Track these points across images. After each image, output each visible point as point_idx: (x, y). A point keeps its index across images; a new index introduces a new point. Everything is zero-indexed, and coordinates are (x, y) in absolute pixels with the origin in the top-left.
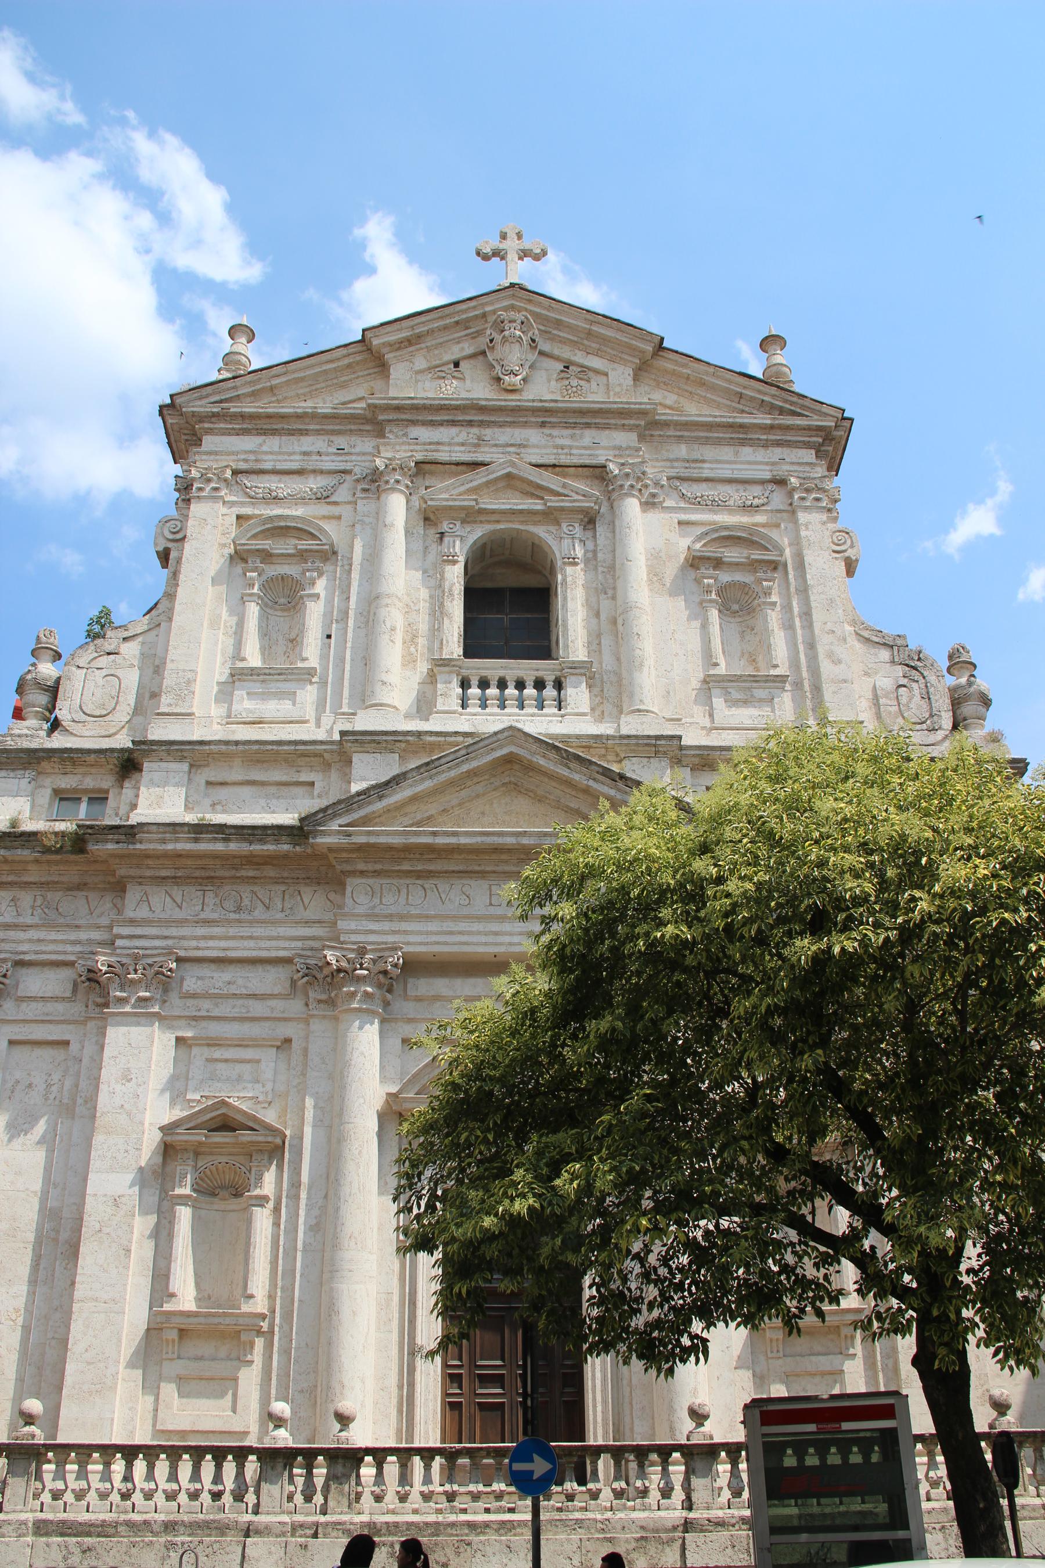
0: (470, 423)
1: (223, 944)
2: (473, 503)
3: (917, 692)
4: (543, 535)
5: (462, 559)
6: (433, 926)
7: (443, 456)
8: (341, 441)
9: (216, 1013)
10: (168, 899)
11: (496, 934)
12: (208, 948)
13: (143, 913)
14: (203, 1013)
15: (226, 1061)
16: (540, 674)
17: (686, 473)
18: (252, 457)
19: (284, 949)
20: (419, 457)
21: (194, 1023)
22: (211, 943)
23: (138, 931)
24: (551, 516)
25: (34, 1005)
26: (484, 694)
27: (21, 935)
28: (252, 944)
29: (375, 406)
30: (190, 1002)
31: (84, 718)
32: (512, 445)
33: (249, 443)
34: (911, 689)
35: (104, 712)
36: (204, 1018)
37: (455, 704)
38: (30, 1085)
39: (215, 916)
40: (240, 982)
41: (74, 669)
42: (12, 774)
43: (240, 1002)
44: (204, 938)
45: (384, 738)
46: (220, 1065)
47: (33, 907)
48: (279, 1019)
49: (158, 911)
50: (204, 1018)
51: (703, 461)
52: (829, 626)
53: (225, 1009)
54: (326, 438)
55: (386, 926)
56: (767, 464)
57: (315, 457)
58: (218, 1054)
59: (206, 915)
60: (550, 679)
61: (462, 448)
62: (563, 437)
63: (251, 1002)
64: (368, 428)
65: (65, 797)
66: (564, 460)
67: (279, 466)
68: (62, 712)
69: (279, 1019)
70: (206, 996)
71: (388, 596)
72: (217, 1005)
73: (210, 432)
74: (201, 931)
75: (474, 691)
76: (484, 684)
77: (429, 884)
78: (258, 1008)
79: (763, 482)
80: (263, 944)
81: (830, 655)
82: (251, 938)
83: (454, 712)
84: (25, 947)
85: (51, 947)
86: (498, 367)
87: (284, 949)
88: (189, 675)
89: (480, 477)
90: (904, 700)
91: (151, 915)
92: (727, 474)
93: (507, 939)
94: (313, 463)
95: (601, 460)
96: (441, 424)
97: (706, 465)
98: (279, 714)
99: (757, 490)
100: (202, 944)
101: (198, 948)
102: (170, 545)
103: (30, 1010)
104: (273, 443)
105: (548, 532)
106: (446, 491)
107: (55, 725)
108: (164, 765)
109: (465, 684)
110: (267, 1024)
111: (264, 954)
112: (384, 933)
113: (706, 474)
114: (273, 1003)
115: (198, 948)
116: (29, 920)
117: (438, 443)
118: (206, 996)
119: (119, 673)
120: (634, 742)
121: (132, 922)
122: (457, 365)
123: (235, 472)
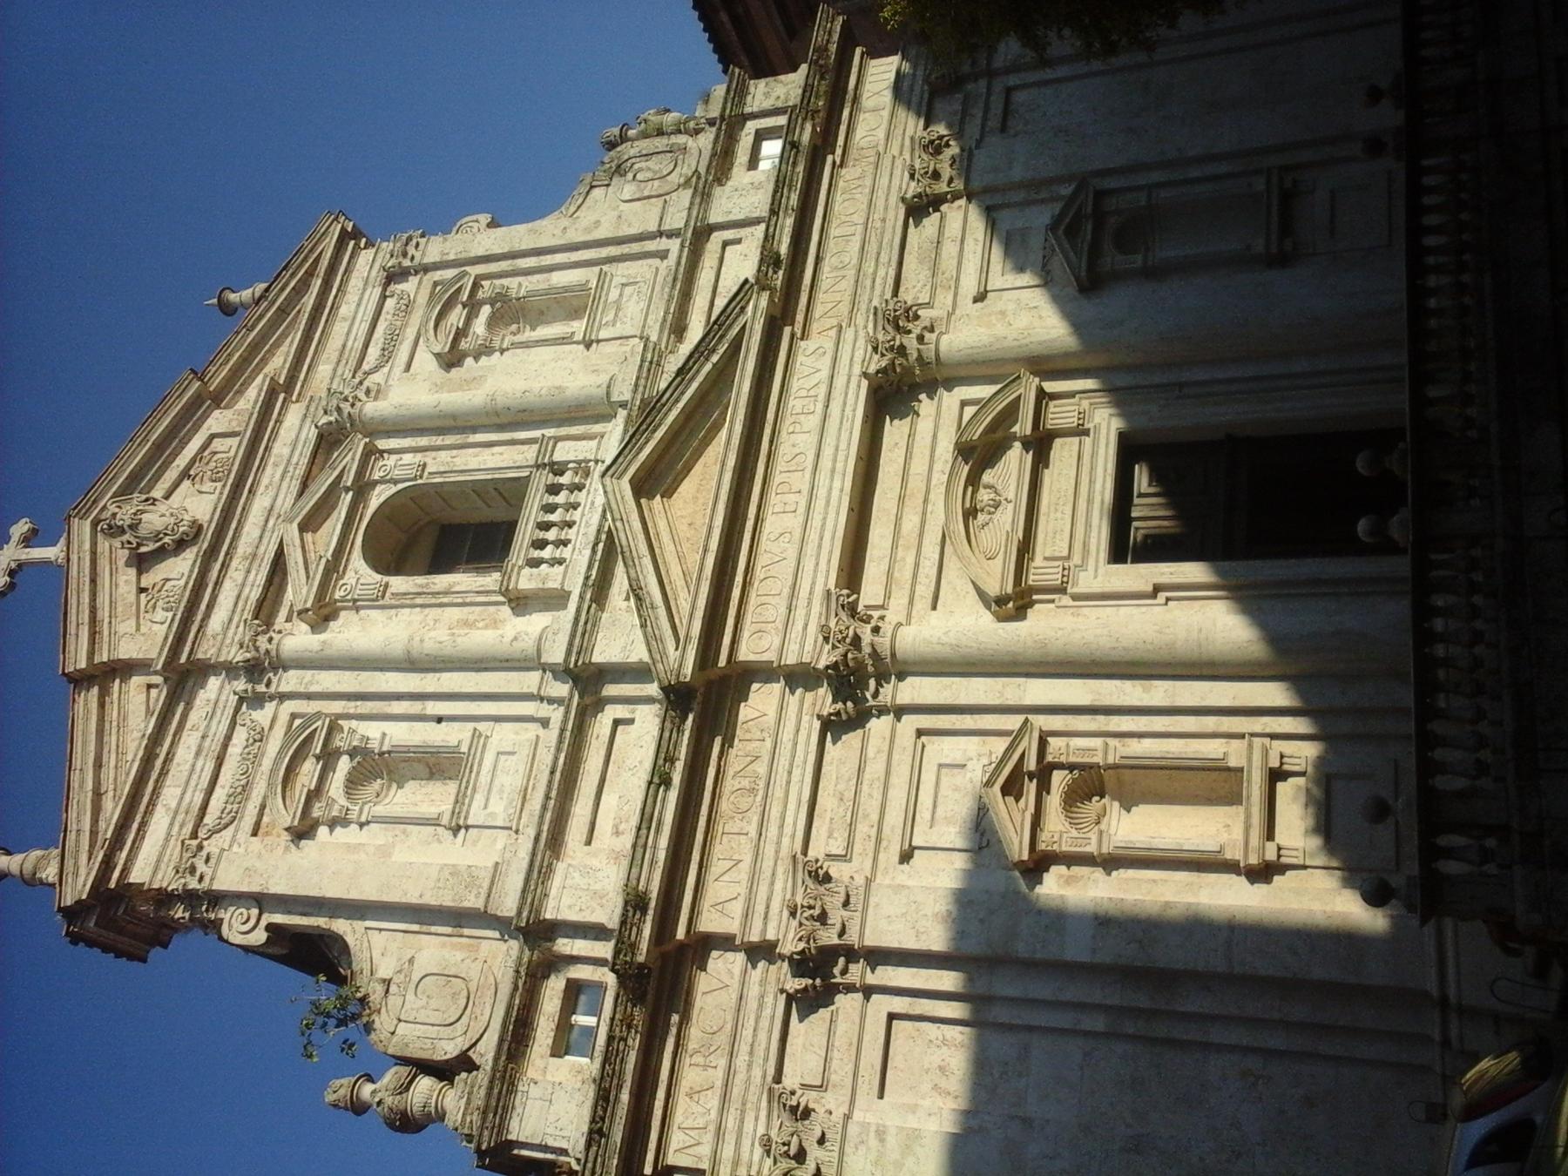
0: (225, 566)
1: (792, 806)
2: (324, 561)
3: (643, 165)
4: (382, 499)
5: (386, 579)
6: (808, 564)
7: (255, 594)
8: (195, 716)
9: (875, 817)
10: (725, 878)
11: (828, 502)
12: (795, 824)
13: (737, 908)
14: (873, 832)
15: (935, 806)
16: (542, 488)
17: (352, 363)
18: (180, 818)
19: (809, 736)
20: (248, 615)
21: (884, 844)
22: (789, 820)
23: (760, 908)
24: (362, 488)
25: (835, 1064)
26: (552, 543)
27: (740, 1079)
28: (796, 772)
29: (167, 664)
30: (857, 848)
31: (465, 1019)
32: (267, 521)
33: (159, 822)
34: (641, 170)
35: (465, 993)
36: (880, 831)
37: (559, 569)
38: (940, 1068)
39: (755, 819)
40: (841, 787)
41: (395, 1039)
42: (519, 1110)
43: (865, 787)
44: (782, 826)
45: (582, 623)
46: (940, 811)
47: (706, 1067)
48: (892, 741)
49: (739, 890)
50: (880, 831)
51: (344, 346)
52: (558, 232)
53: (870, 805)
54: (185, 733)
55: (800, 614)
56: (364, 290)
57: (208, 740)
58: (924, 814)
59: (753, 830)
60: (551, 479)
61: (253, 572)
62: (271, 474)
63: (867, 776)
64: (190, 683)
65: (561, 1048)
66: (301, 471)
67: (204, 783)
68: (448, 1049)
69: (892, 741)
70: (852, 826)
71: (411, 639)
72: (866, 816)
73: (126, 870)
74: (772, 831)
75: (547, 553)
76: (540, 544)
77: (759, 573)
78: (875, 769)
79: (383, 298)
80: (799, 759)
81: (588, 230)
82: (790, 773)
83: (566, 572)
84: (757, 1073)
85: (762, 1036)
86: (167, 540)
87: (809, 736)
88: (446, 873)
89: (294, 558)
90: (649, 175)
91: (741, 900)
92: (365, 326)
93: (835, 493)
94: (213, 746)
95: (314, 433)
96: (214, 598)
97: (350, 344)
98: (521, 770)
99: (390, 304)
100: (788, 830)
101: (793, 836)
102: (263, 923)
103: (841, 1070)
104: (170, 794)
105: (379, 495)
106: (299, 591)
107: (464, 1063)
108: (553, 892)
109: (535, 563)
110: (895, 757)
111: (812, 758)
112: (808, 615)
113: (359, 345)
114: (871, 752)
115: (793, 836)
116: (720, 1074)
117: (238, 597)
118: (852, 826)
119: (415, 978)
120: (642, 381)
121: (746, 915)
122: (142, 590)
123: (194, 835)
